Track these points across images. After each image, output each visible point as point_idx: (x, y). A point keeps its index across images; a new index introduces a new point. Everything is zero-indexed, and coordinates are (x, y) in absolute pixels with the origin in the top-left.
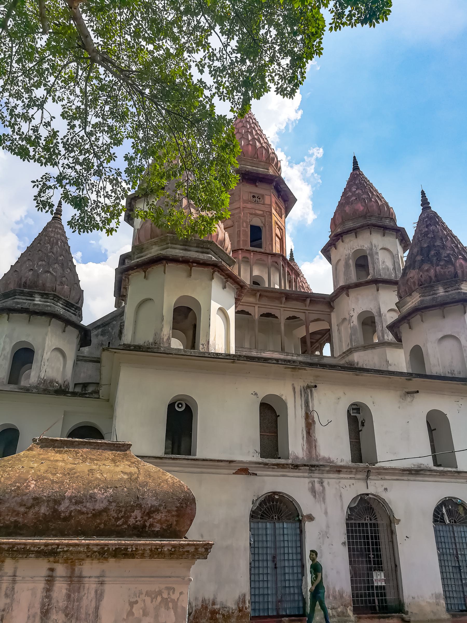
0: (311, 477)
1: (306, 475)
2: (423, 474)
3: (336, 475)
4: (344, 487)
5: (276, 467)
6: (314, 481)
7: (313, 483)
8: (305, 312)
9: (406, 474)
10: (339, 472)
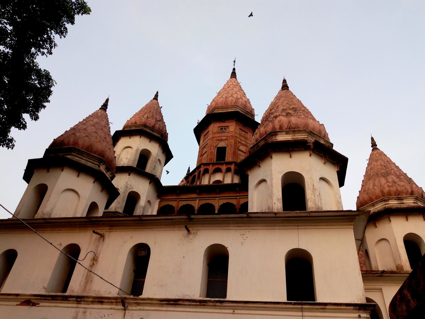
0: (77, 307)
1: (75, 305)
2: (181, 304)
3: (99, 306)
4: (103, 316)
5: (50, 298)
6: (79, 311)
7: (77, 313)
8: (236, 198)
9: (164, 304)
10: (101, 303)
